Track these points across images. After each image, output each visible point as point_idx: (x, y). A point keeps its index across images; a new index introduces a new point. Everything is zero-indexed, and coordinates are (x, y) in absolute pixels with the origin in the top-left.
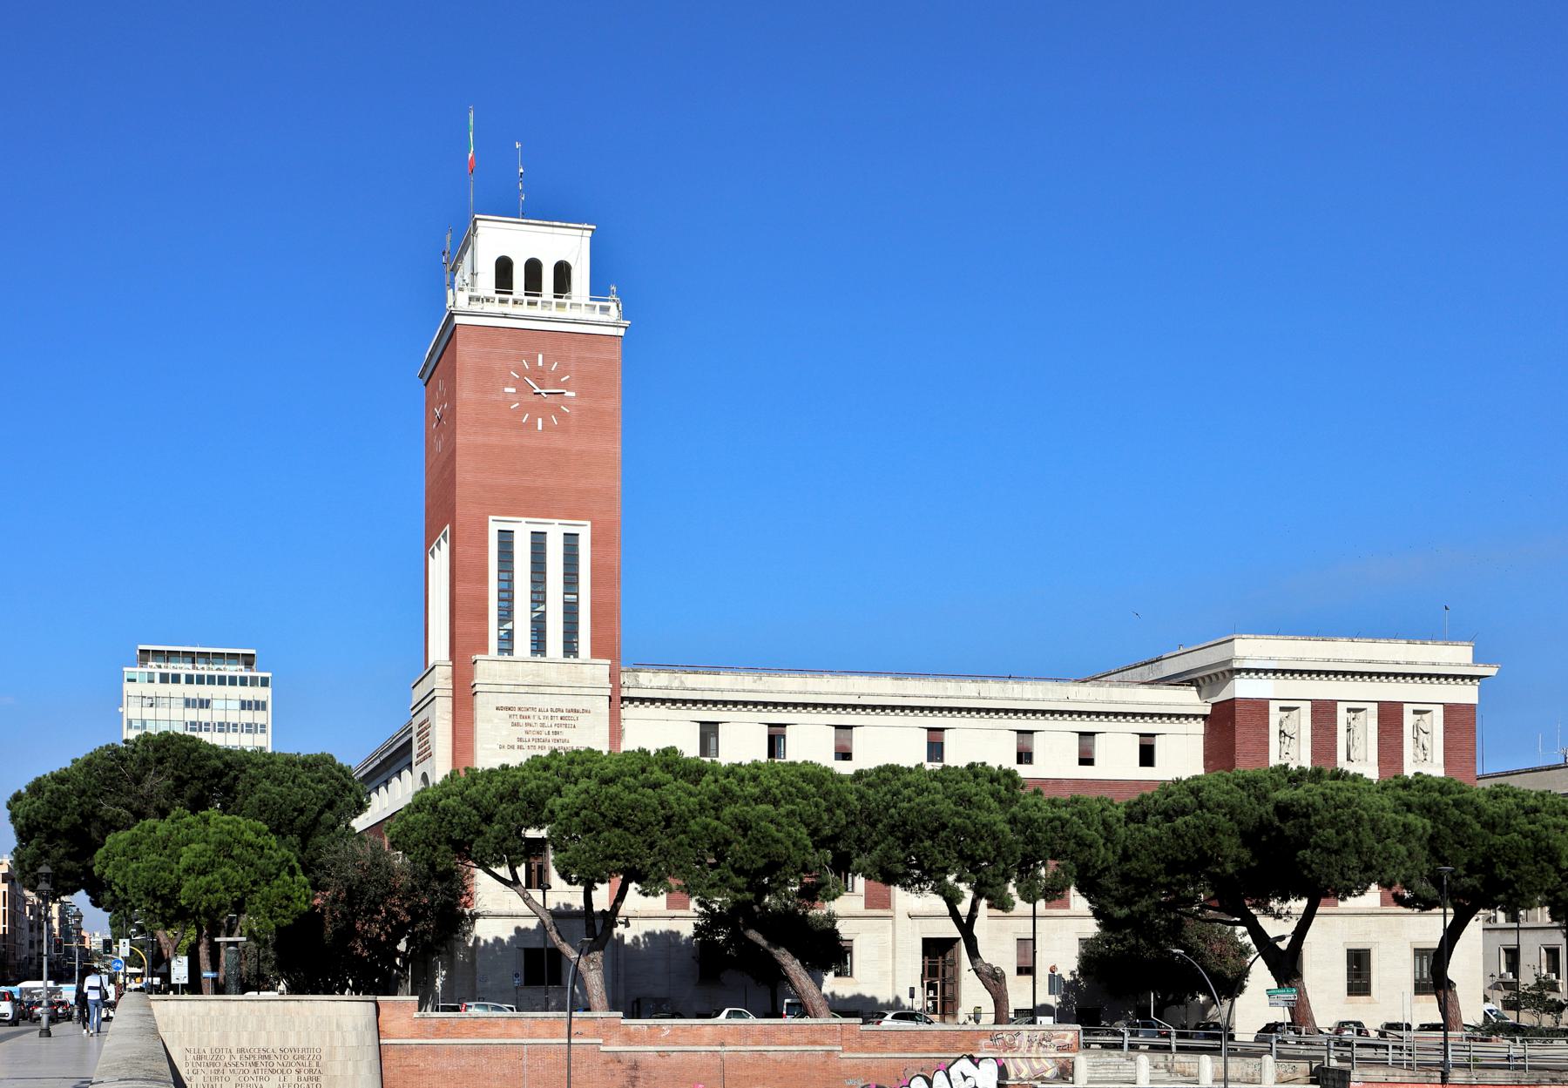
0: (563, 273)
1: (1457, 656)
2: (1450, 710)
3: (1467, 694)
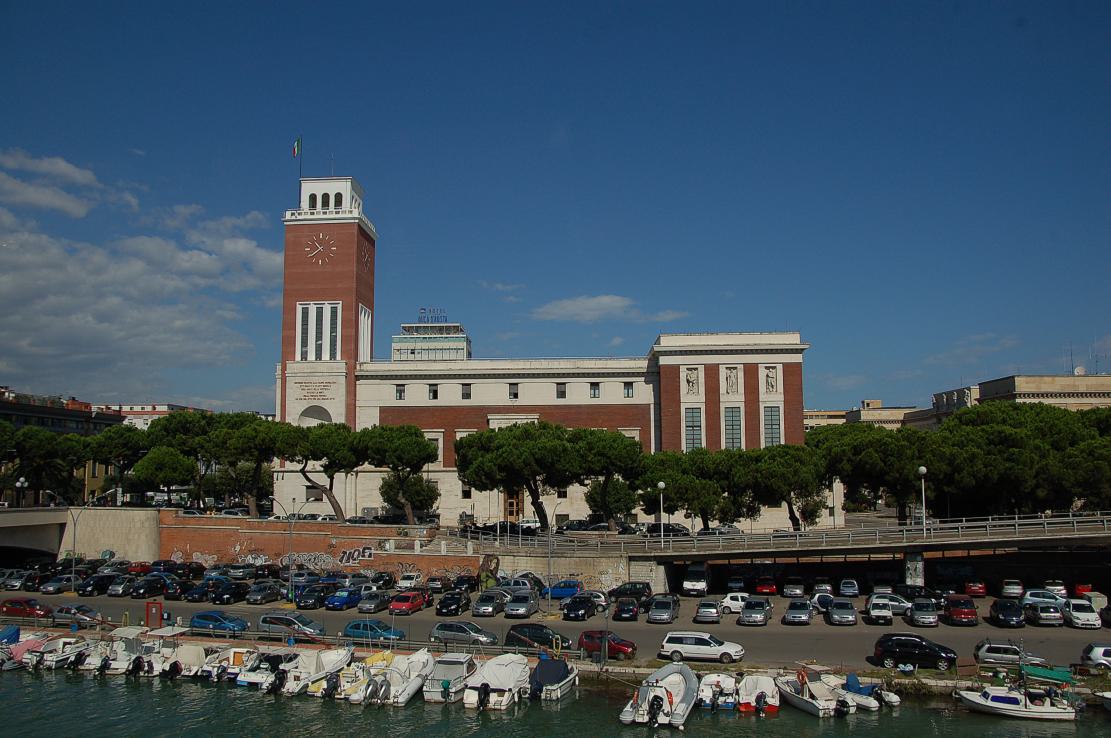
0: (339, 197)
1: (792, 339)
2: (786, 366)
3: (797, 358)
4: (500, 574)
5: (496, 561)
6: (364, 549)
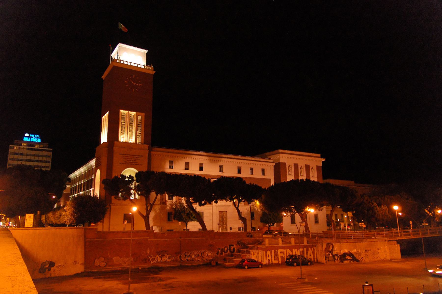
4: (335, 253)
5: (331, 246)
6: (230, 246)
